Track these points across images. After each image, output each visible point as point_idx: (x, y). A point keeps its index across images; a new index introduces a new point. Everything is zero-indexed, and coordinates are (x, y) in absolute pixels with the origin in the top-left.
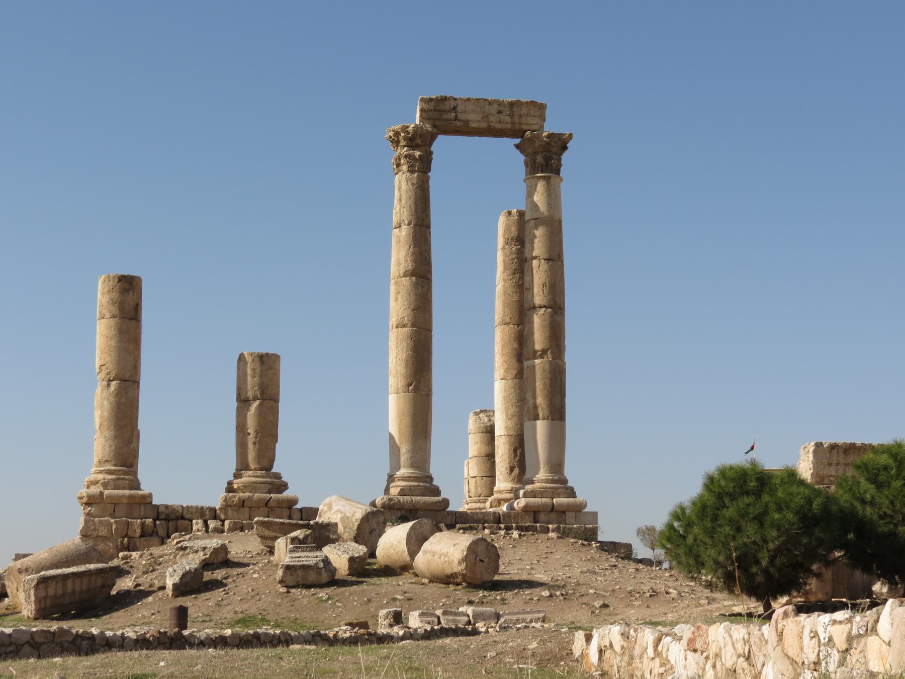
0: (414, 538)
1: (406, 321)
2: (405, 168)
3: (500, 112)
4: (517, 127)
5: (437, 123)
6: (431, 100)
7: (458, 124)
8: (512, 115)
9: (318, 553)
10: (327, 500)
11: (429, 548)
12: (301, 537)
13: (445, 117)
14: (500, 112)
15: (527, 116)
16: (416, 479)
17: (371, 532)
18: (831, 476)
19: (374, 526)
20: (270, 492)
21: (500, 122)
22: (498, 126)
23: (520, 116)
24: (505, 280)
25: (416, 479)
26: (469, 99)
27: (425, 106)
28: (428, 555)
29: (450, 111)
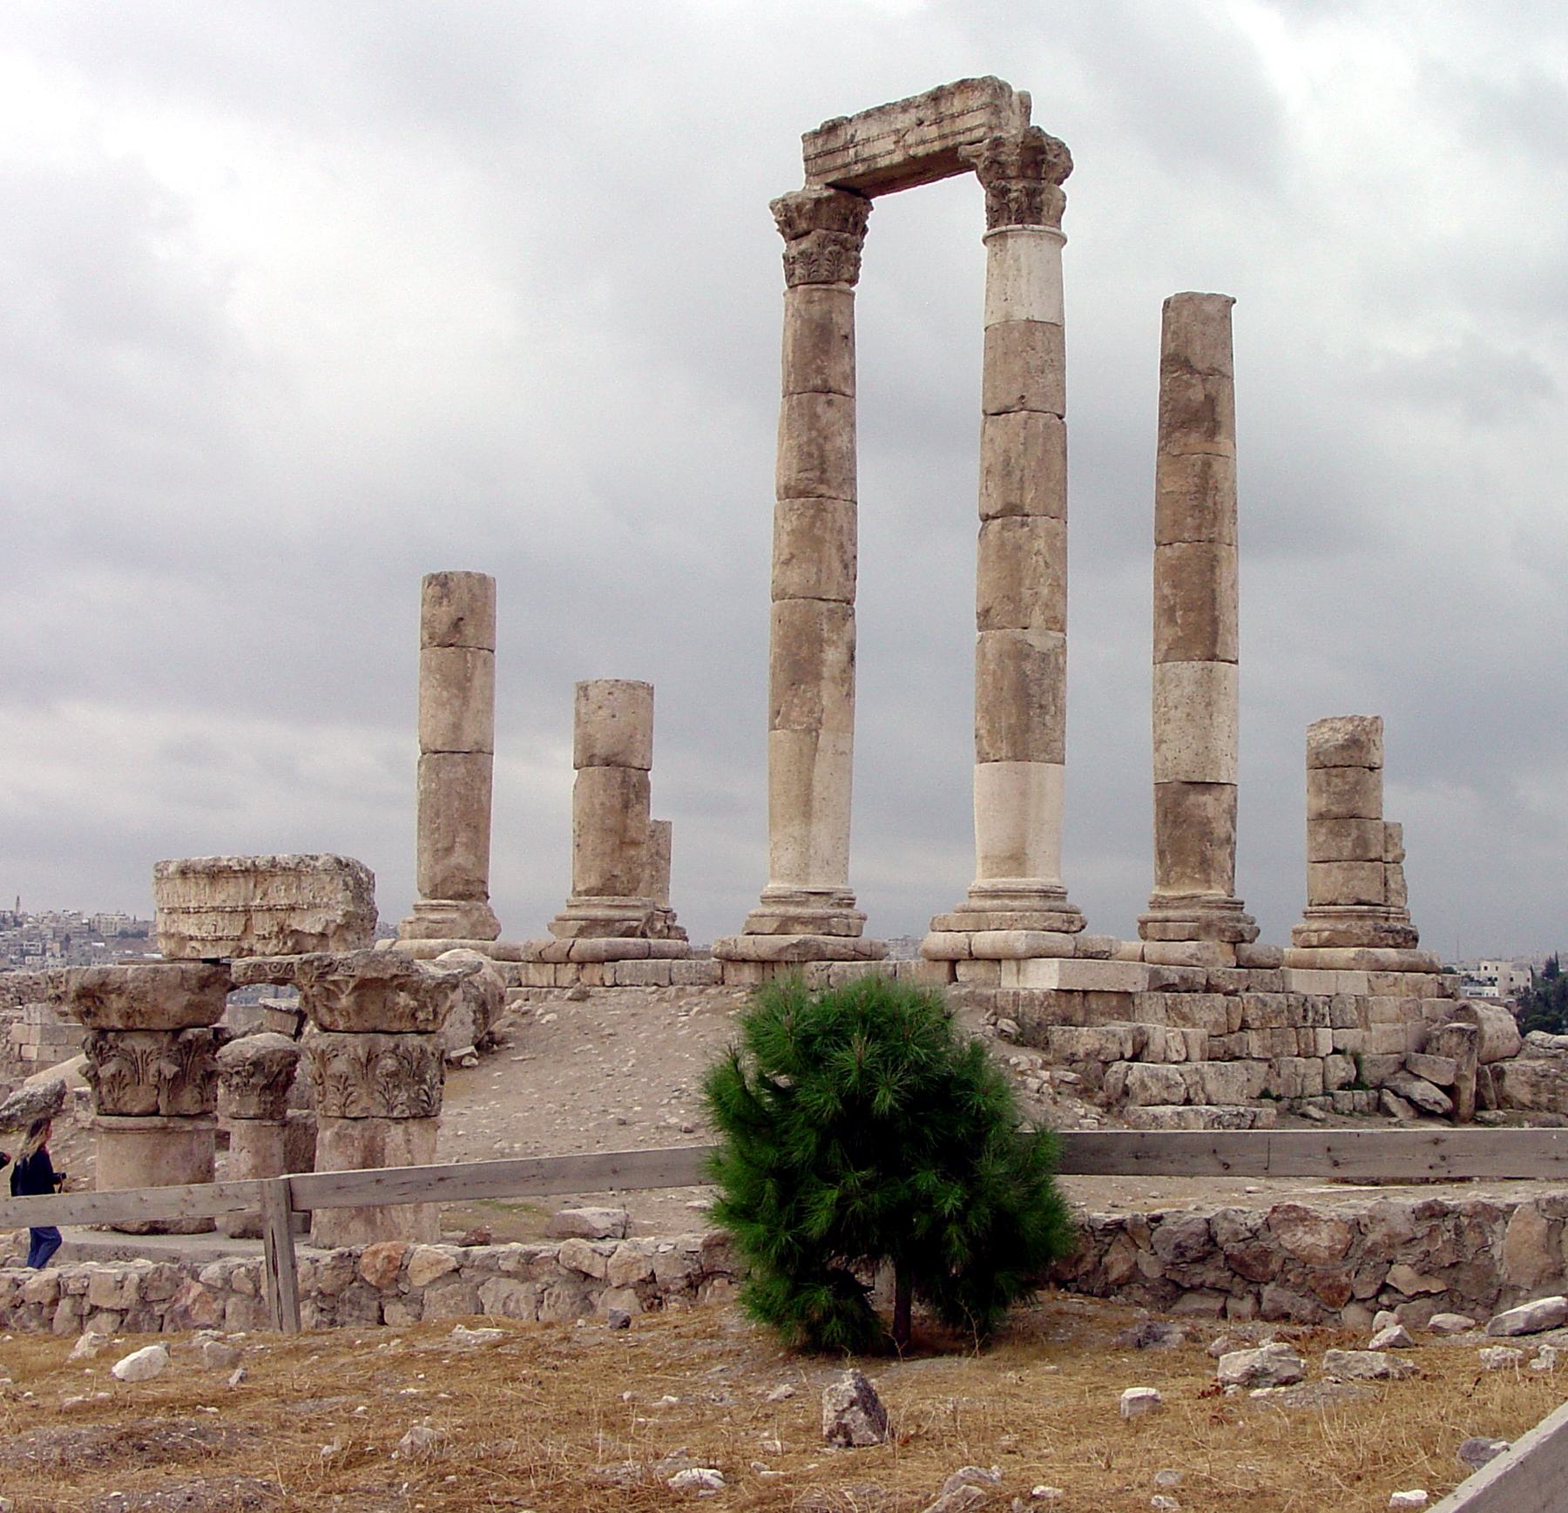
3: (920, 123)
4: (950, 142)
5: (832, 178)
6: (816, 134)
7: (860, 168)
8: (938, 121)
13: (839, 162)
14: (920, 123)
15: (962, 114)
18: (191, 938)
21: (923, 142)
22: (921, 151)
23: (952, 116)
25: (779, 899)
26: (868, 115)
27: (812, 151)
29: (845, 148)
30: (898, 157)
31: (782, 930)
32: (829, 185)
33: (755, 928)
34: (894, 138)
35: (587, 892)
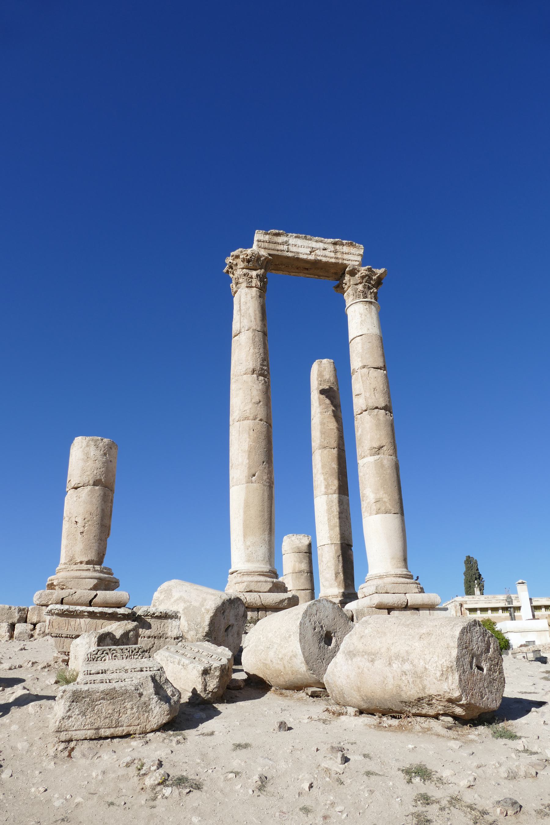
0: (310, 632)
1: (248, 415)
2: (244, 285)
4: (340, 261)
7: (290, 255)
8: (336, 252)
9: (145, 662)
10: (165, 585)
11: (360, 647)
12: (118, 635)
16: (262, 574)
17: (227, 630)
19: (232, 621)
20: (95, 588)
22: (324, 259)
23: (343, 253)
24: (321, 413)
25: (262, 574)
28: (358, 660)
30: (312, 257)
31: (270, 591)
32: (270, 255)
33: (252, 588)
34: (310, 250)
35: (88, 563)
